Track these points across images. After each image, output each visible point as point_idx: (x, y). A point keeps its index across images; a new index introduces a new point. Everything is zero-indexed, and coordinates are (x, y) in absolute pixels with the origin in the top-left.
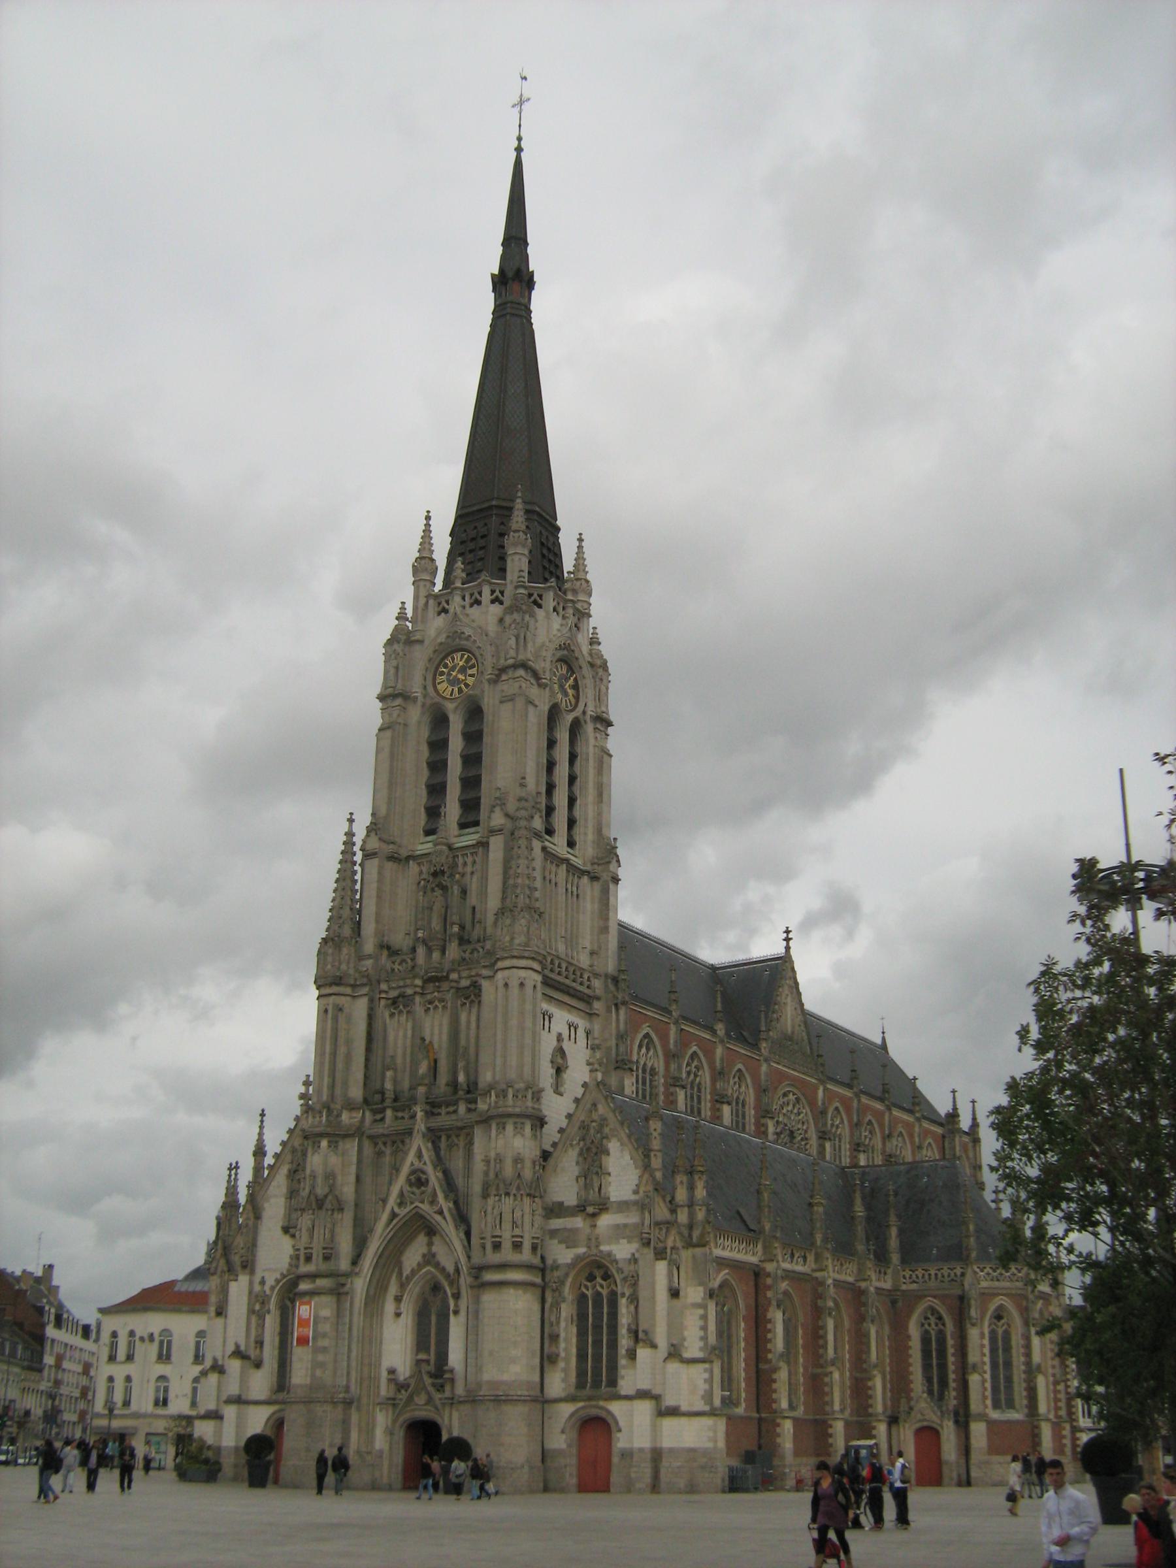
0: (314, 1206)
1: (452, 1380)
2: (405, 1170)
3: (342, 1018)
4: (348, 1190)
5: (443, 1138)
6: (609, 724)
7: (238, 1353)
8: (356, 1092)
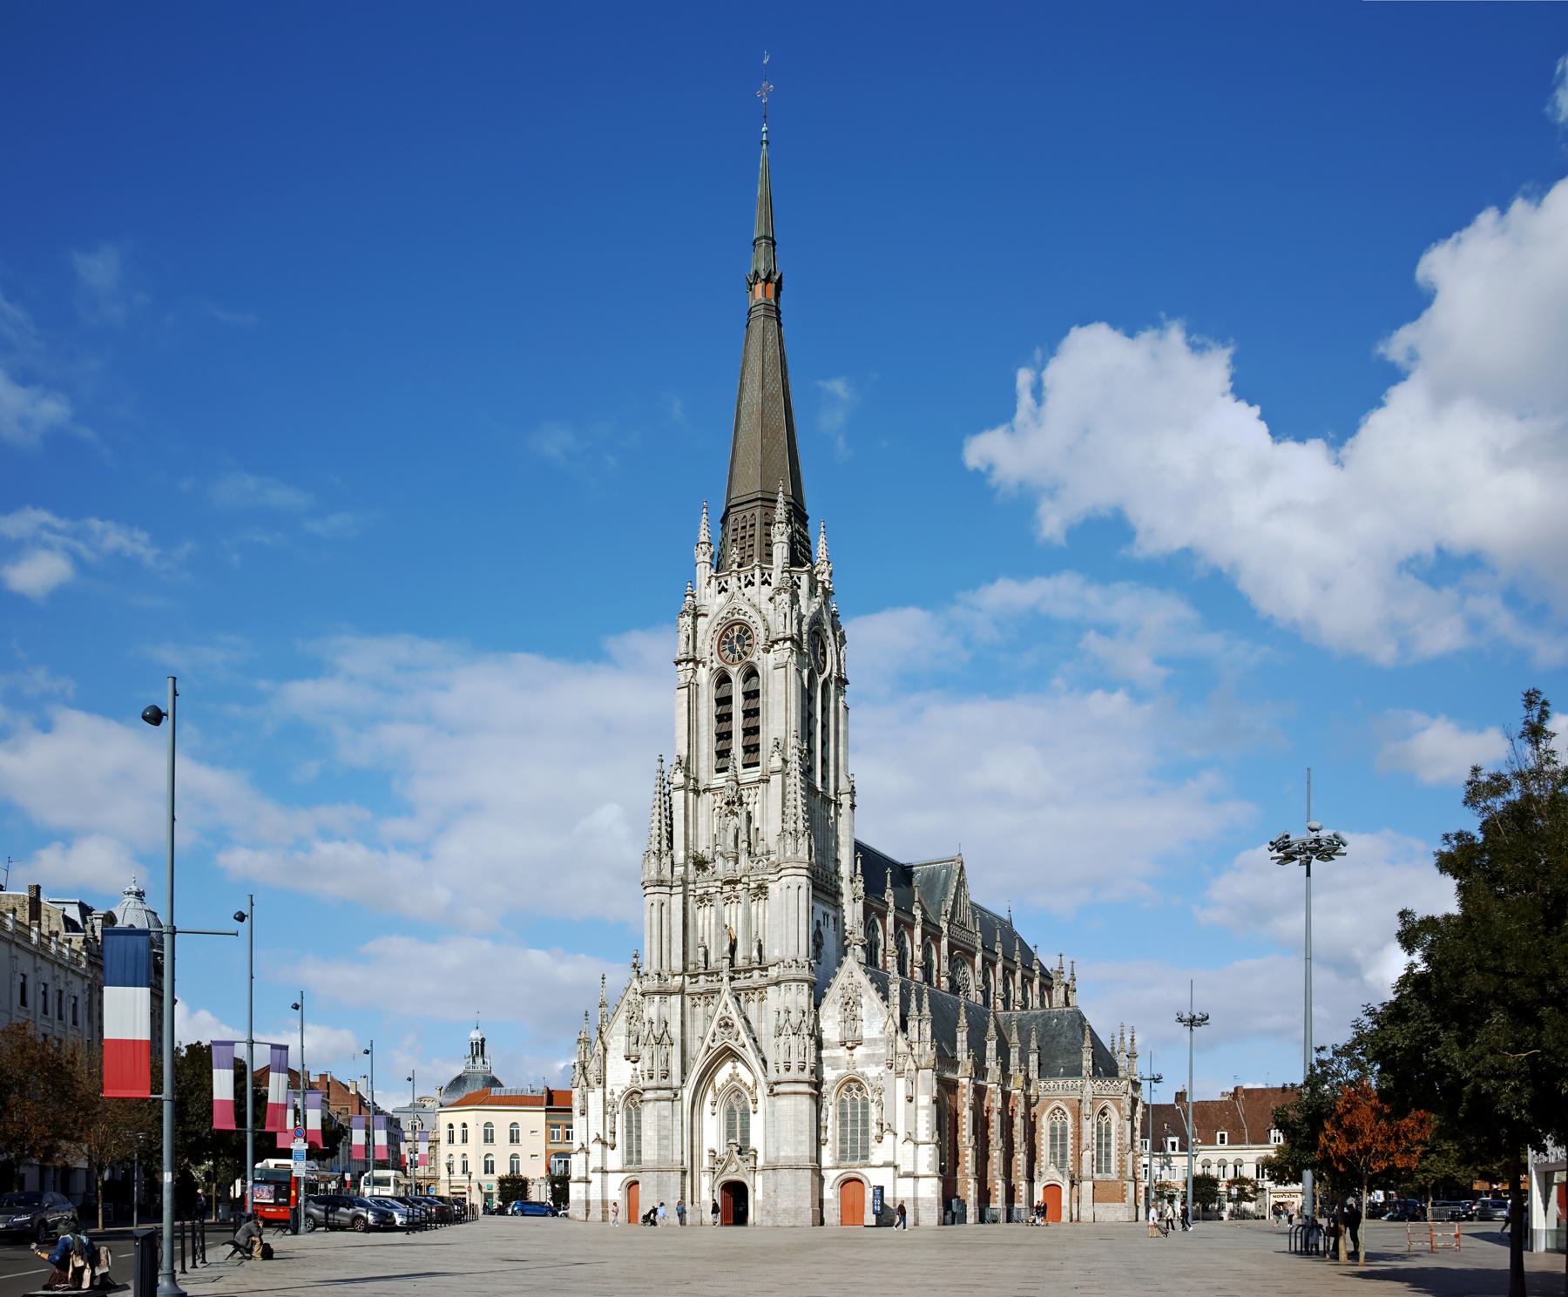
0: (653, 1042)
1: (755, 1157)
2: (717, 1018)
4: (675, 1030)
5: (743, 995)
7: (598, 1139)
8: (677, 964)
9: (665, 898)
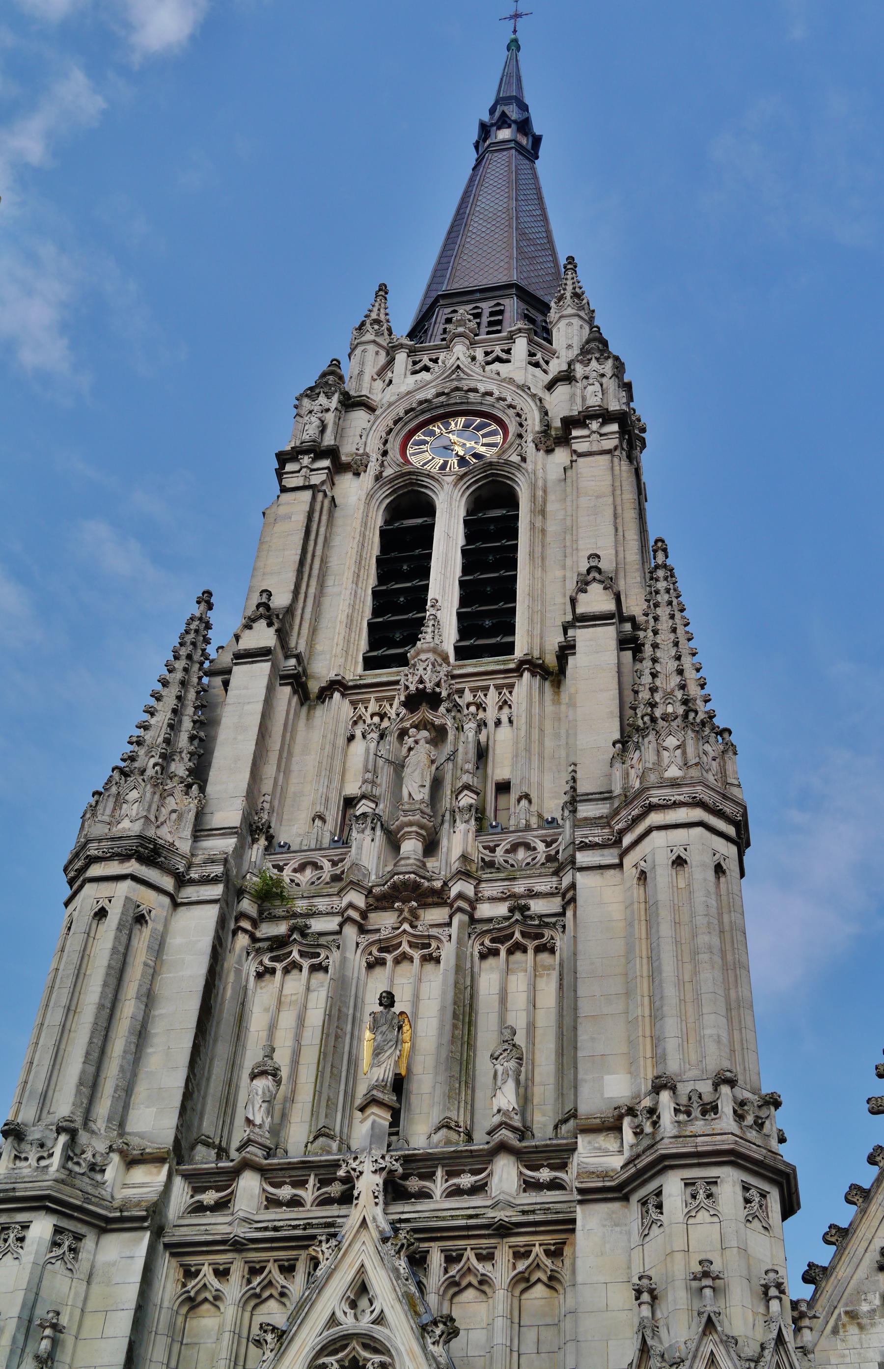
3: (143, 939)
9: (149, 899)
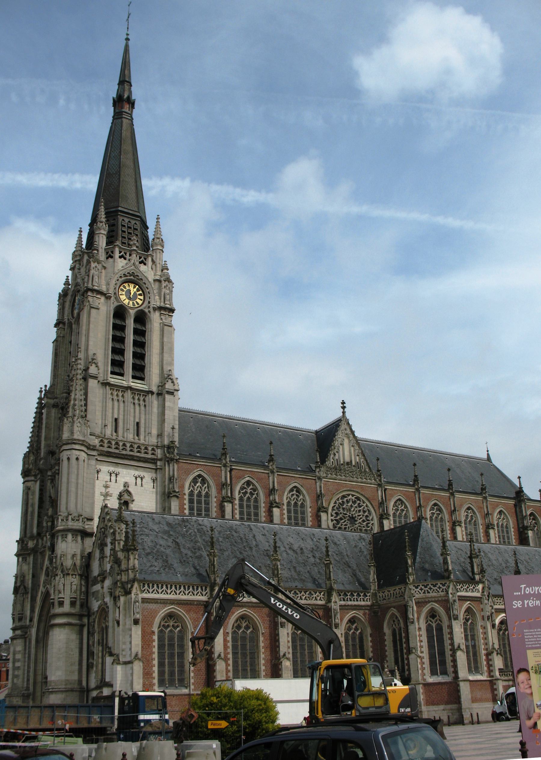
6: (172, 310)
